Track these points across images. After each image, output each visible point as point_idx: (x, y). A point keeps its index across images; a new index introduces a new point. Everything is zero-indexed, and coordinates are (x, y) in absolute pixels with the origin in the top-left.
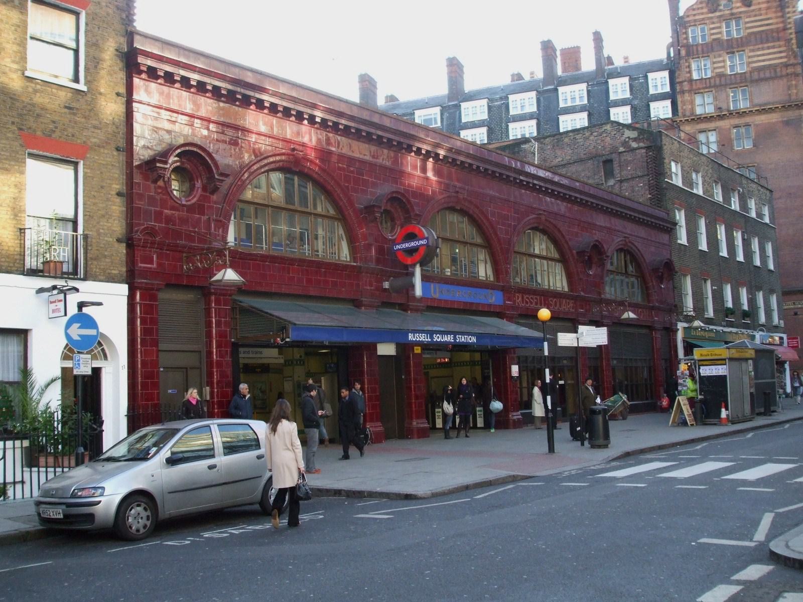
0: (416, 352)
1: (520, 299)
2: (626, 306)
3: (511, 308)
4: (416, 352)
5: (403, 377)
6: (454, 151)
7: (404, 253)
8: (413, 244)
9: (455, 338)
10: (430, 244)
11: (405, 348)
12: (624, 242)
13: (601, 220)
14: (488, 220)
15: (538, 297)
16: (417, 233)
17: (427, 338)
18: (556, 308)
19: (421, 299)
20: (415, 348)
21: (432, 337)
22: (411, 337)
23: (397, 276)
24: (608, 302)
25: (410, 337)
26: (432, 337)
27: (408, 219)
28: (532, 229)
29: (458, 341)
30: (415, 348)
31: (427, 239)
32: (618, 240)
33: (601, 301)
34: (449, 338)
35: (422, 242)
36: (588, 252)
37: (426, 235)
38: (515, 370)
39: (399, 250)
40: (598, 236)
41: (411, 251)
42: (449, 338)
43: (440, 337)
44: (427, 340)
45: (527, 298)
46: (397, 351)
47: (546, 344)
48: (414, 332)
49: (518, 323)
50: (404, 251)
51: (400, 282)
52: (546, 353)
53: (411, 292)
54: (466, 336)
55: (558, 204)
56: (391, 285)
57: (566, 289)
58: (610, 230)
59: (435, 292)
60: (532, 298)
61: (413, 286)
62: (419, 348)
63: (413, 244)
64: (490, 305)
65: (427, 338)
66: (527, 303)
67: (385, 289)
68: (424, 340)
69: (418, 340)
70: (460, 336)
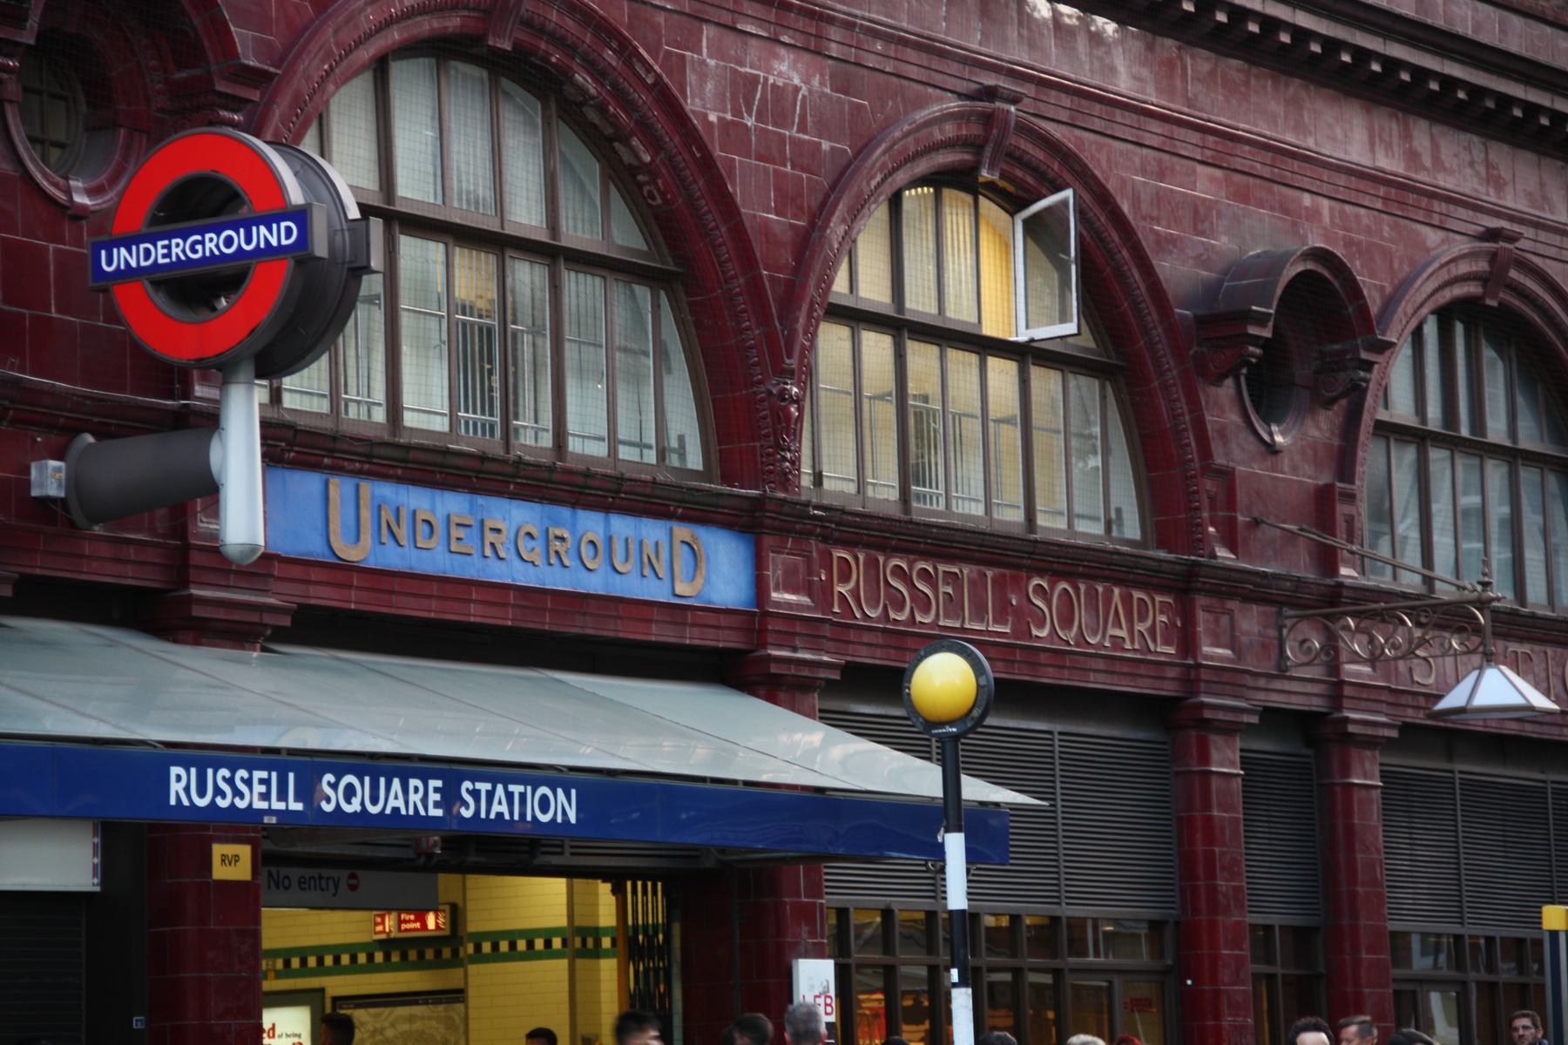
0: (220, 872)
1: (858, 574)
2: (1478, 630)
3: (794, 627)
4: (220, 872)
5: (138, 1022)
7: (160, 300)
8: (212, 243)
9: (450, 797)
10: (321, 249)
11: (152, 847)
12: (1482, 266)
13: (1348, 136)
14: (679, 117)
15: (967, 571)
16: (235, 178)
17: (283, 796)
18: (1070, 635)
19: (266, 566)
20: (218, 850)
21: (307, 791)
22: (180, 785)
23: (115, 425)
24: (1377, 607)
25: (176, 788)
26: (307, 791)
27: (196, 104)
28: (938, 180)
29: (467, 813)
30: (218, 850)
31: (301, 216)
32: (1444, 255)
33: (1329, 602)
34: (415, 798)
35: (276, 236)
36: (1261, 320)
37: (296, 196)
38: (814, 979)
39: (129, 272)
40: (1323, 224)
41: (197, 287)
42: (415, 798)
43: (363, 790)
44: (278, 805)
46: (107, 868)
47: (955, 844)
49: (831, 718)
50: (157, 284)
51: (132, 462)
52: (957, 897)
53: (204, 524)
54: (516, 789)
55: (1097, 38)
56: (74, 482)
57: (1132, 529)
58: (1402, 196)
60: (924, 574)
61: (209, 490)
62: (244, 851)
63: (212, 243)
65: (283, 796)
67: (46, 501)
68: (260, 805)
69: (223, 803)
70: (484, 787)
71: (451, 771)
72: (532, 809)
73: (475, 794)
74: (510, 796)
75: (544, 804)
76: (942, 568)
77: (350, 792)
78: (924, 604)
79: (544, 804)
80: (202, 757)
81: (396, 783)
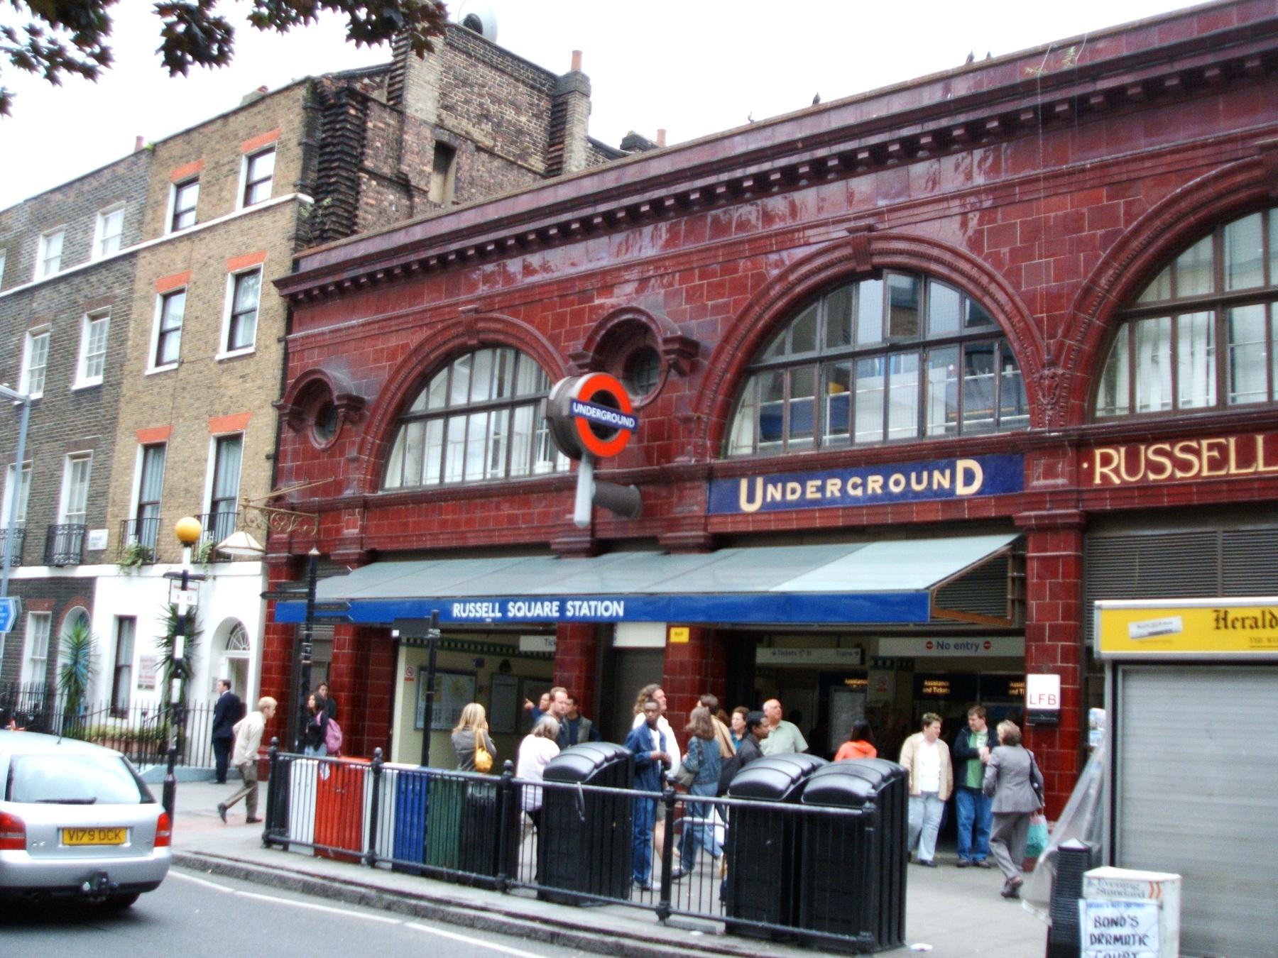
6: (800, 145)
9: (562, 609)
26: (504, 609)
29: (569, 614)
44: (492, 615)
45: (1159, 452)
48: (465, 600)
54: (593, 603)
59: (751, 499)
60: (1186, 449)
64: (961, 500)
66: (1159, 469)
68: (485, 615)
69: (472, 615)
70: (577, 603)
71: (563, 600)
72: (601, 612)
73: (574, 607)
74: (590, 607)
75: (607, 609)
76: (1205, 443)
77: (519, 609)
78: (1186, 466)
79: (607, 609)
80: (465, 600)
81: (539, 604)
